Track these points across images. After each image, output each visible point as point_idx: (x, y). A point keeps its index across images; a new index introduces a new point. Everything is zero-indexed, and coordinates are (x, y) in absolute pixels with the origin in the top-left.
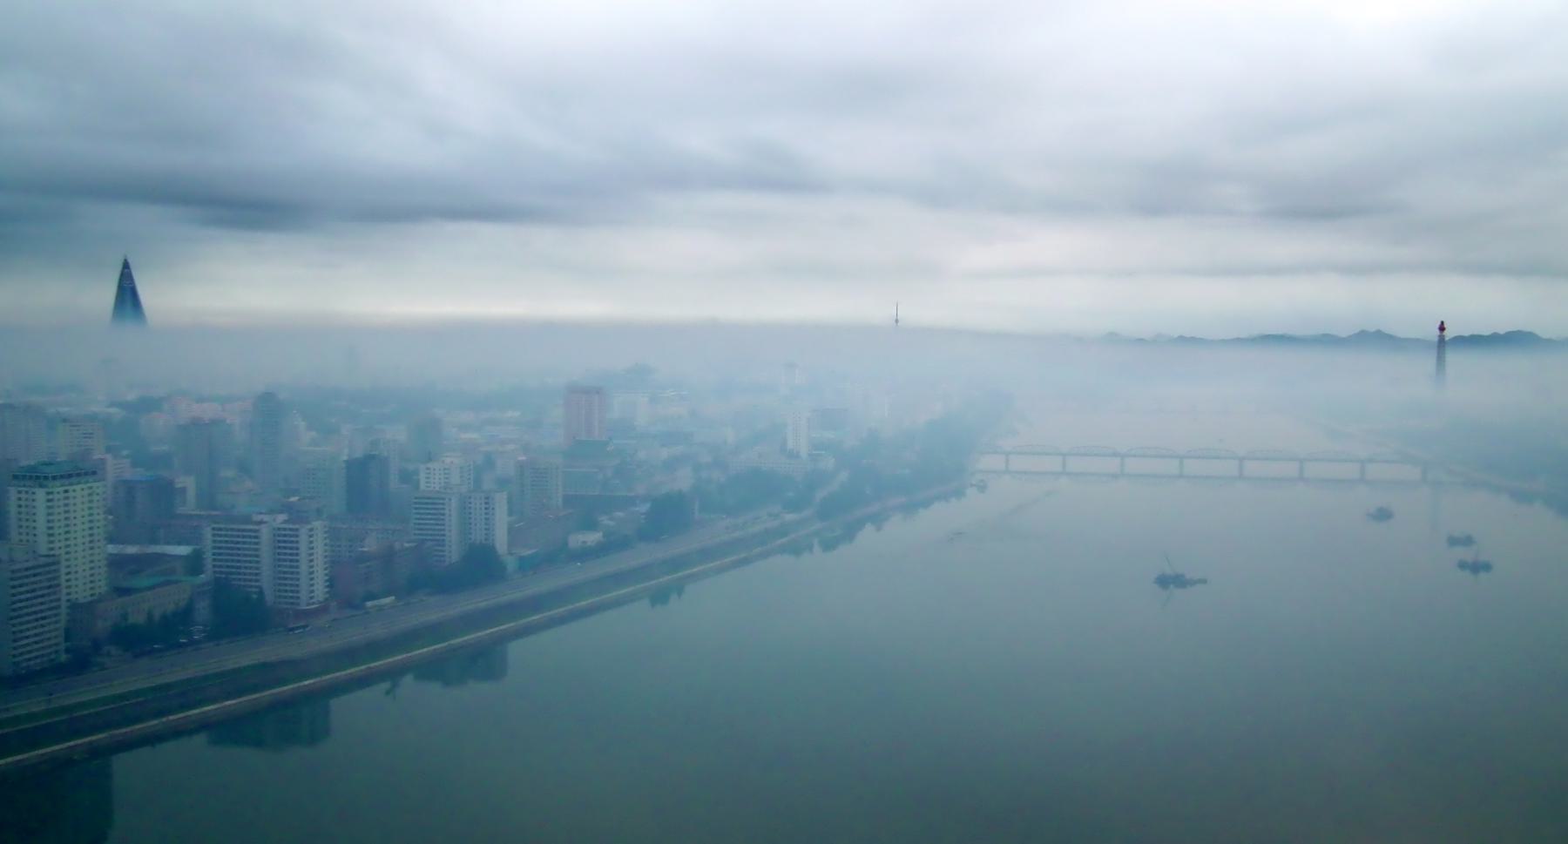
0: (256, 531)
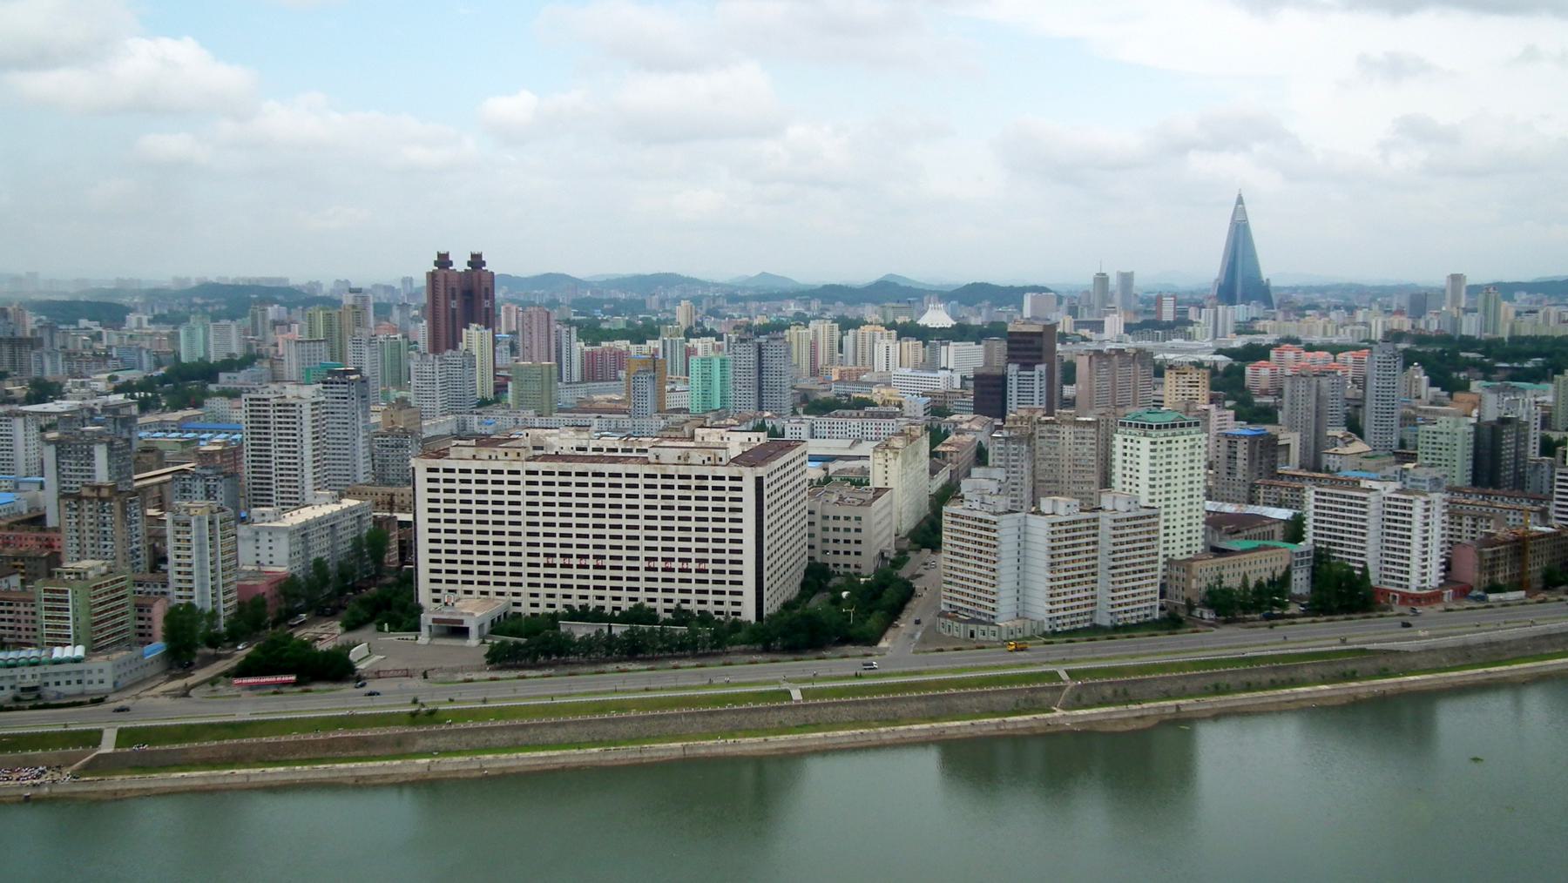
0: (1364, 499)
